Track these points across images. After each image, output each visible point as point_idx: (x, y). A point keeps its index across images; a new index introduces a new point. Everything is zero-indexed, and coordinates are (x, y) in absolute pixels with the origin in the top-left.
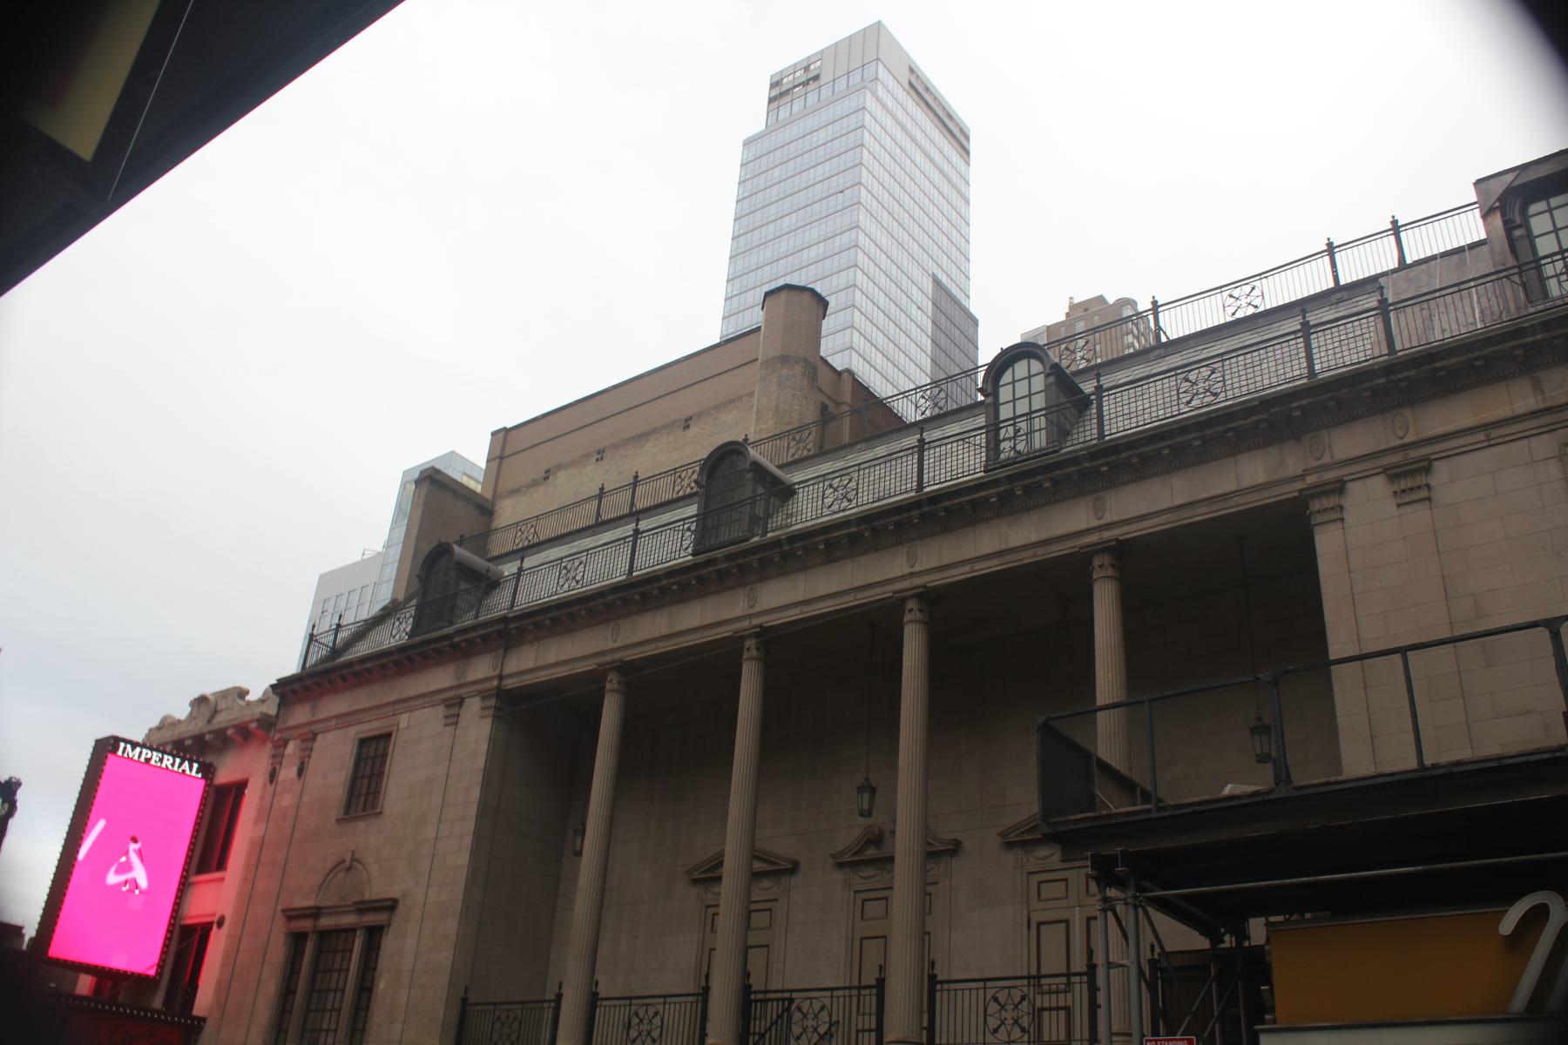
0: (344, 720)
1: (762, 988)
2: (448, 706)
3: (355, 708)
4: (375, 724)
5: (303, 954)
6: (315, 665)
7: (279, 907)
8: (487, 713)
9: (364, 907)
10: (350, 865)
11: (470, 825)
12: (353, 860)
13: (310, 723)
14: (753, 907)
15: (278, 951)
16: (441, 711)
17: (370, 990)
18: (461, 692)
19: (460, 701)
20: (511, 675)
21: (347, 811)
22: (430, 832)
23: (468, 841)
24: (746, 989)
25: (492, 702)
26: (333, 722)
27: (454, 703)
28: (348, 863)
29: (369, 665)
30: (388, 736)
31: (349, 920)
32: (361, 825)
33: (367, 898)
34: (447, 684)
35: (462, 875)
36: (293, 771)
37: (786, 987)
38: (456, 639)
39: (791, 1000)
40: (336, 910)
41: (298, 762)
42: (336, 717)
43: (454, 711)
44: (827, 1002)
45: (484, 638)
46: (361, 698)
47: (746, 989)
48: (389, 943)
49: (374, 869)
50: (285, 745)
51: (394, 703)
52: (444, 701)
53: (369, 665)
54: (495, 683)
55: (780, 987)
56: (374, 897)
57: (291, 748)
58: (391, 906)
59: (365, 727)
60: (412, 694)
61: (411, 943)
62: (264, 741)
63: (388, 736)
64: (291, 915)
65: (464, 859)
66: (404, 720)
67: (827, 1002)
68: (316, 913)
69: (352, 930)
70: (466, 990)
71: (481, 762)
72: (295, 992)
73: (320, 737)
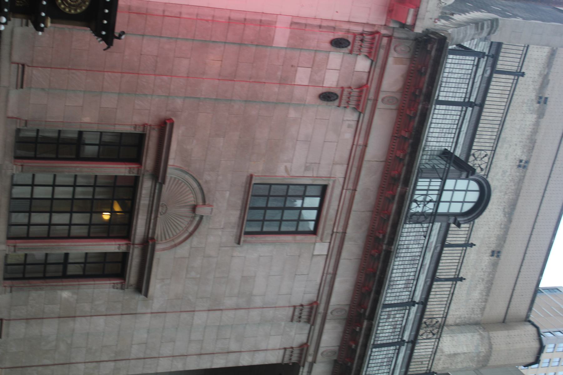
0: (356, 161)
16: (311, 296)
19: (310, 320)
25: (294, 359)
26: (361, 142)
27: (310, 313)
28: (201, 211)
32: (234, 216)
33: (158, 247)
36: (331, 81)
38: (365, 323)
42: (365, 145)
45: (355, 351)
46: (369, 180)
49: (183, 250)
50: (368, 56)
51: (344, 233)
53: (394, 207)
54: (310, 359)
56: (157, 254)
57: (362, 64)
58: (141, 287)
59: (337, 191)
60: (344, 254)
62: (390, 12)
66: (321, 248)
68: (158, 175)
73: (355, 116)
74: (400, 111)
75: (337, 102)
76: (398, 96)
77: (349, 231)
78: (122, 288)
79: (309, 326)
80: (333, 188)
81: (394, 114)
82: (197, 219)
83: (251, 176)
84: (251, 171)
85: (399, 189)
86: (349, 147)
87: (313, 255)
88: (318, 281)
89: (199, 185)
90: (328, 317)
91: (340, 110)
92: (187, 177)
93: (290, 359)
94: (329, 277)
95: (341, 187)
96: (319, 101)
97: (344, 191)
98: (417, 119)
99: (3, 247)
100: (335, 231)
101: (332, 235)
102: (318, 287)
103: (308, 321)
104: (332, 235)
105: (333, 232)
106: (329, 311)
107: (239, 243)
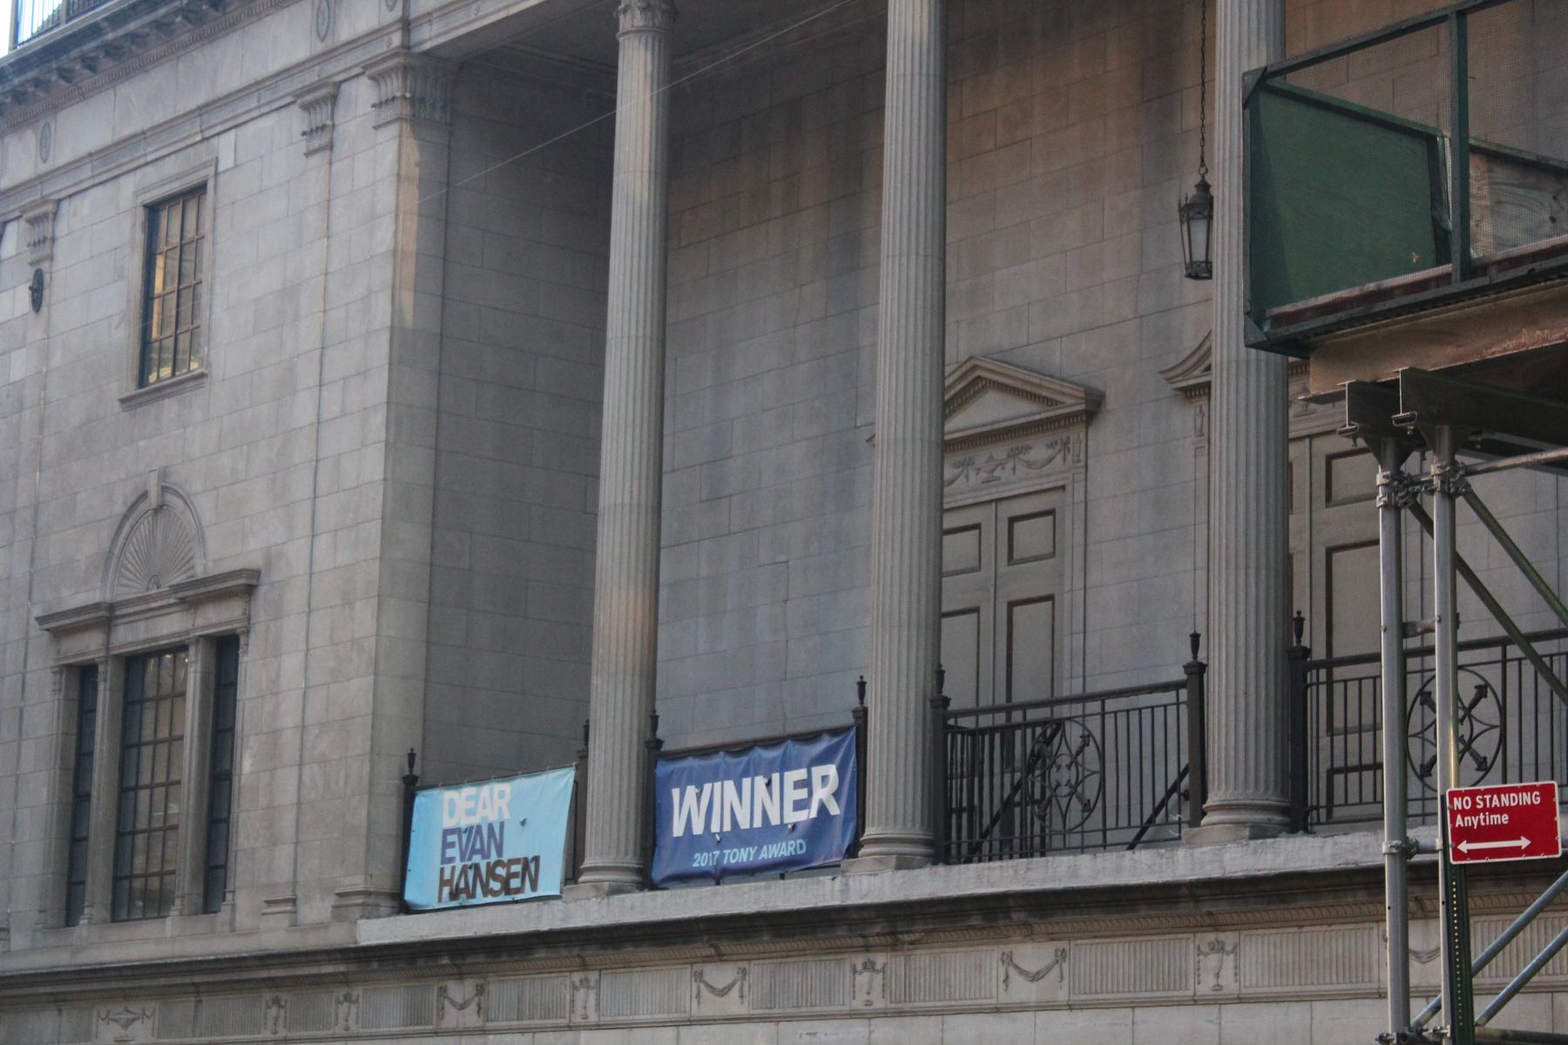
1: (969, 704)
2: (307, 107)
3: (127, 131)
4: (171, 167)
5: (94, 711)
6: (54, 21)
7: (37, 611)
8: (389, 113)
9: (197, 595)
10: (155, 505)
11: (377, 388)
12: (164, 490)
13: (41, 179)
14: (950, 521)
15: (45, 712)
16: (296, 120)
17: (228, 776)
18: (330, 68)
20: (428, 17)
21: (142, 381)
22: (303, 410)
23: (378, 419)
24: (939, 704)
25: (394, 87)
26: (86, 172)
28: (153, 499)
29: (132, 26)
30: (199, 190)
31: (171, 626)
33: (199, 573)
34: (302, 54)
35: (374, 503)
37: (1092, 688)
39: (1059, 725)
40: (145, 609)
41: (29, 273)
43: (321, 117)
44: (1493, 675)
47: (939, 704)
48: (252, 669)
49: (205, 506)
51: (202, 110)
52: (298, 95)
53: (132, 26)
54: (396, 39)
55: (1077, 690)
59: (151, 174)
60: (234, 83)
61: (292, 663)
63: (199, 190)
64: (60, 627)
65: (371, 466)
67: (1493, 675)
68: (105, 617)
69: (179, 648)
70: (412, 756)
71: (384, 237)
72: (87, 796)
73: (65, 206)
74: (55, 108)
75: (45, 266)
76: (41, 124)
77: (191, 106)
78: (248, 632)
79: (344, 86)
80: (145, 190)
81: (62, 115)
82: (169, 497)
83: (123, 401)
84: (117, 407)
85: (110, 36)
86: (99, 189)
87: (236, 166)
88: (275, 114)
89: (125, 518)
90: (330, 43)
91: (61, 250)
92: (116, 552)
93: (394, 98)
94: (267, 96)
95: (149, 169)
96: (44, 309)
97: (149, 158)
98: (31, 74)
99: (169, 921)
100: (199, 138)
101: (208, 139)
102: (283, 113)
103: (333, 99)
104: (208, 139)
105: (204, 140)
106: (320, 47)
107: (202, 376)
